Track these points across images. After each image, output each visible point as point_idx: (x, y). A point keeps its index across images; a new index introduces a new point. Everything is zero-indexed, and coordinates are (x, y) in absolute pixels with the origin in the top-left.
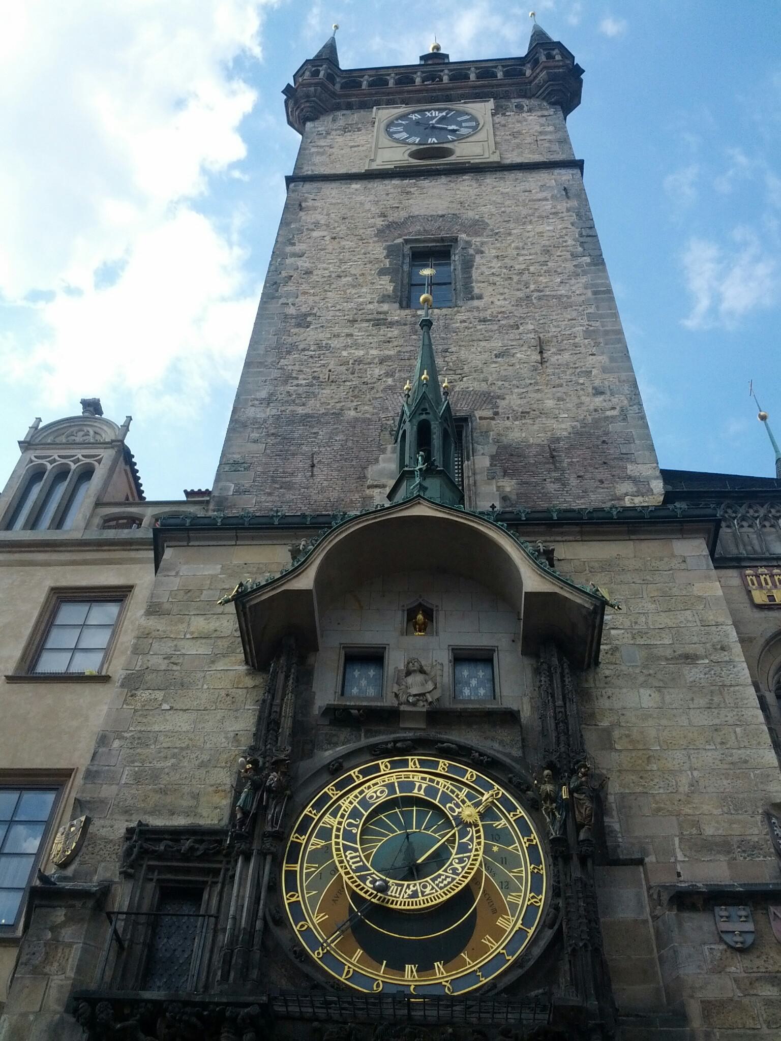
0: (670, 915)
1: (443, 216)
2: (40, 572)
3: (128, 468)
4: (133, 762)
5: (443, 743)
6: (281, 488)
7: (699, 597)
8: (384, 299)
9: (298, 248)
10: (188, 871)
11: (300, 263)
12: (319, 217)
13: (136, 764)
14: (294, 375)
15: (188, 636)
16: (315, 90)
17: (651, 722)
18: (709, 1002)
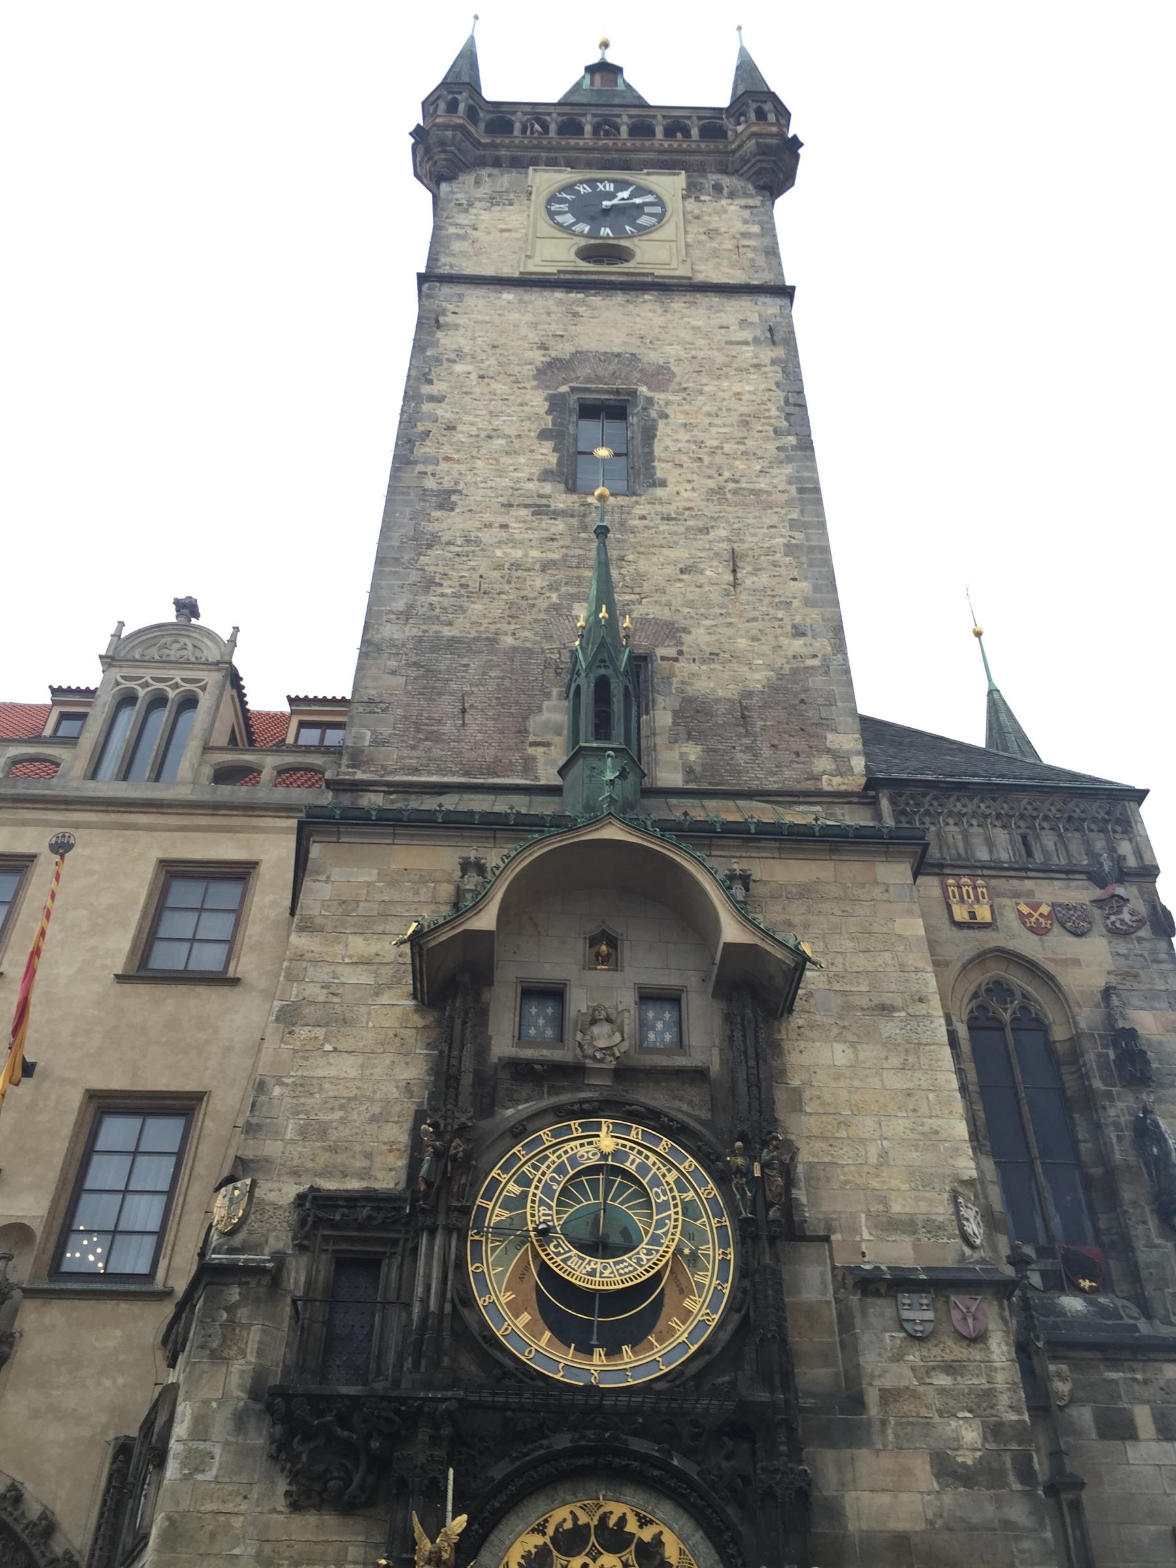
0: (855, 1299)
1: (618, 355)
2: (145, 838)
3: (235, 693)
4: (297, 1113)
5: (631, 1105)
6: (427, 739)
7: (900, 936)
8: (546, 475)
10: (364, 1241)
11: (440, 412)
12: (462, 342)
13: (301, 1116)
14: (437, 580)
15: (347, 960)
16: (454, 136)
17: (842, 1083)
18: (886, 1390)
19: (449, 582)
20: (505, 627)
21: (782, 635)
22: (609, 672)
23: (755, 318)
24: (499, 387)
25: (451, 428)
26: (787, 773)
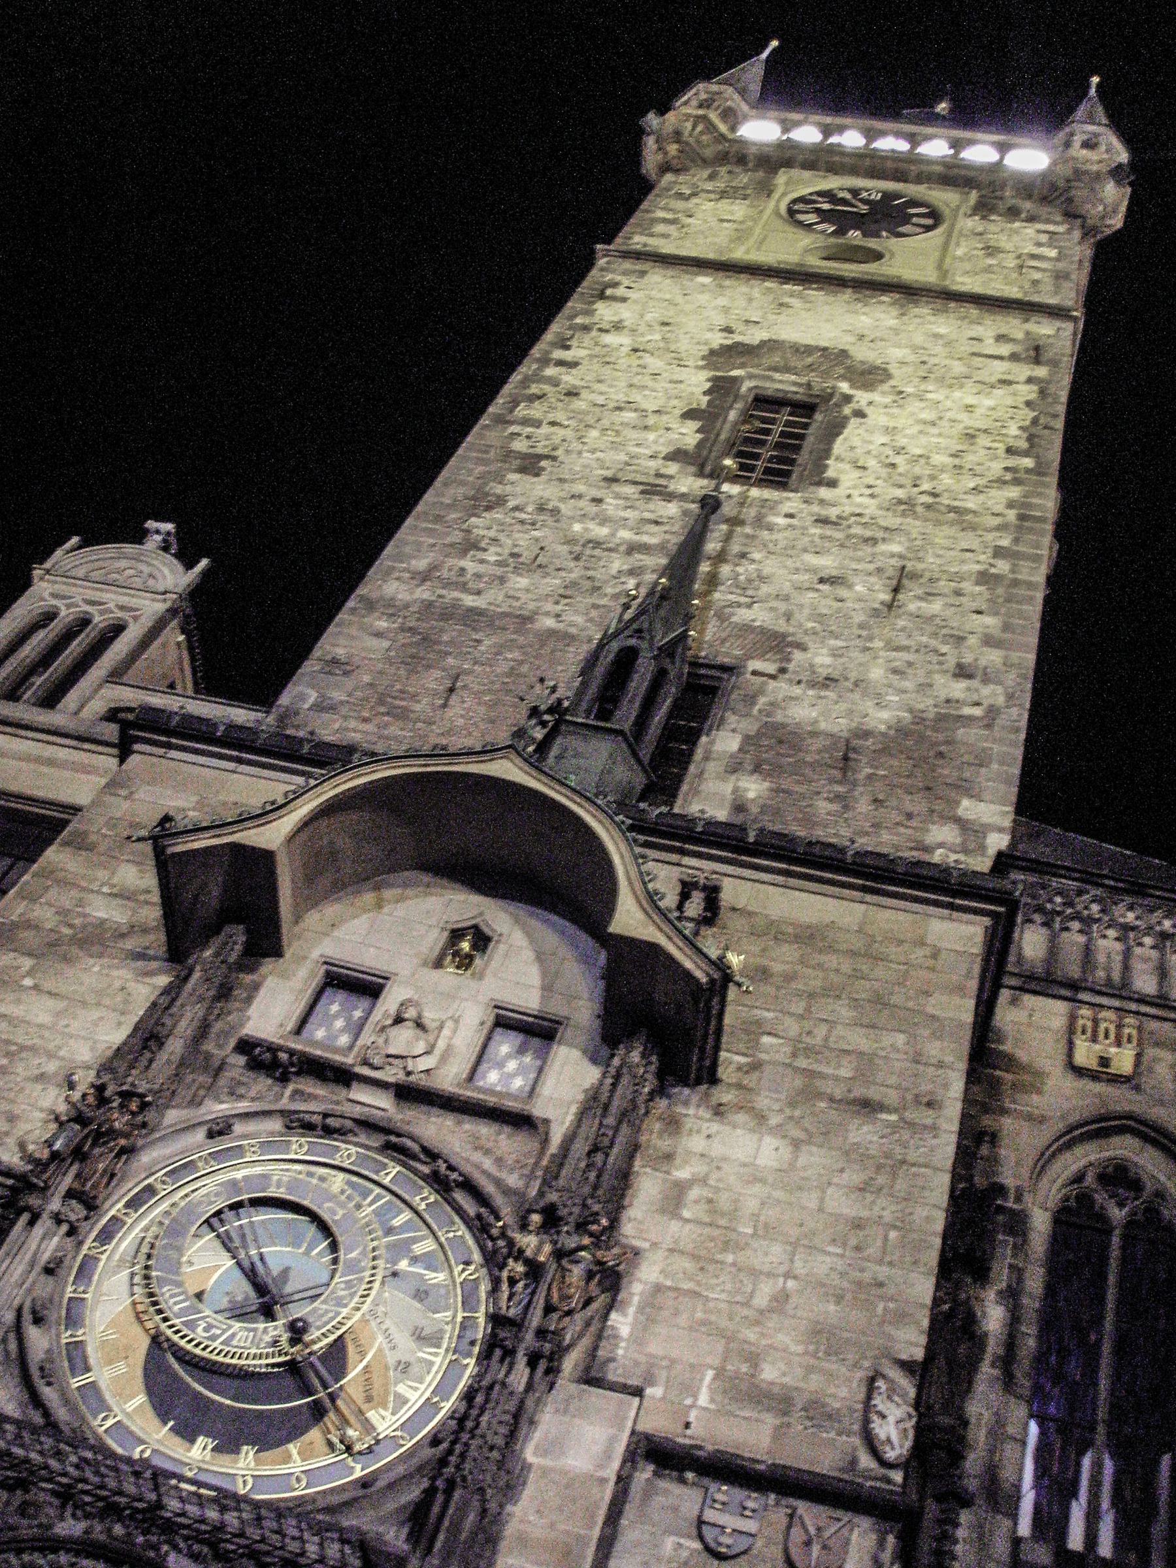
1: (825, 349)
5: (399, 1135)
6: (388, 714)
7: (933, 1016)
9: (567, 355)
11: (565, 378)
14: (483, 545)
15: (105, 889)
17: (757, 1189)
19: (499, 550)
20: (549, 607)
21: (938, 672)
22: (644, 645)
23: (1020, 336)
24: (654, 363)
25: (572, 394)
26: (885, 836)
